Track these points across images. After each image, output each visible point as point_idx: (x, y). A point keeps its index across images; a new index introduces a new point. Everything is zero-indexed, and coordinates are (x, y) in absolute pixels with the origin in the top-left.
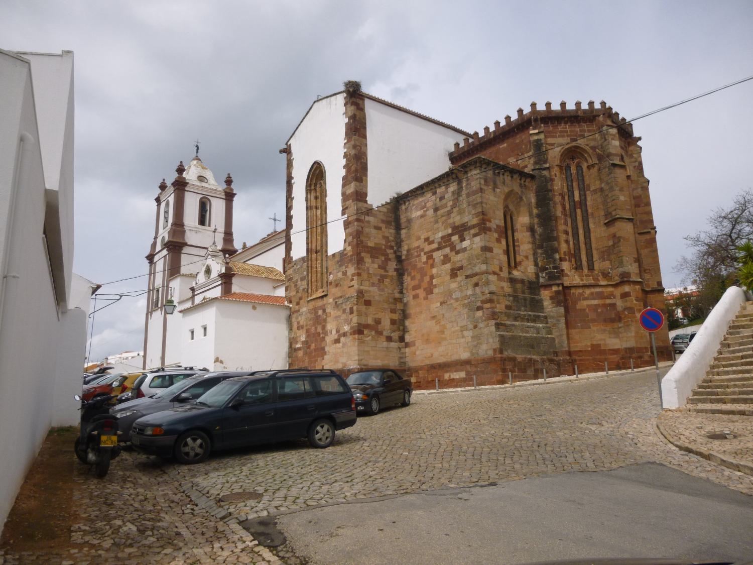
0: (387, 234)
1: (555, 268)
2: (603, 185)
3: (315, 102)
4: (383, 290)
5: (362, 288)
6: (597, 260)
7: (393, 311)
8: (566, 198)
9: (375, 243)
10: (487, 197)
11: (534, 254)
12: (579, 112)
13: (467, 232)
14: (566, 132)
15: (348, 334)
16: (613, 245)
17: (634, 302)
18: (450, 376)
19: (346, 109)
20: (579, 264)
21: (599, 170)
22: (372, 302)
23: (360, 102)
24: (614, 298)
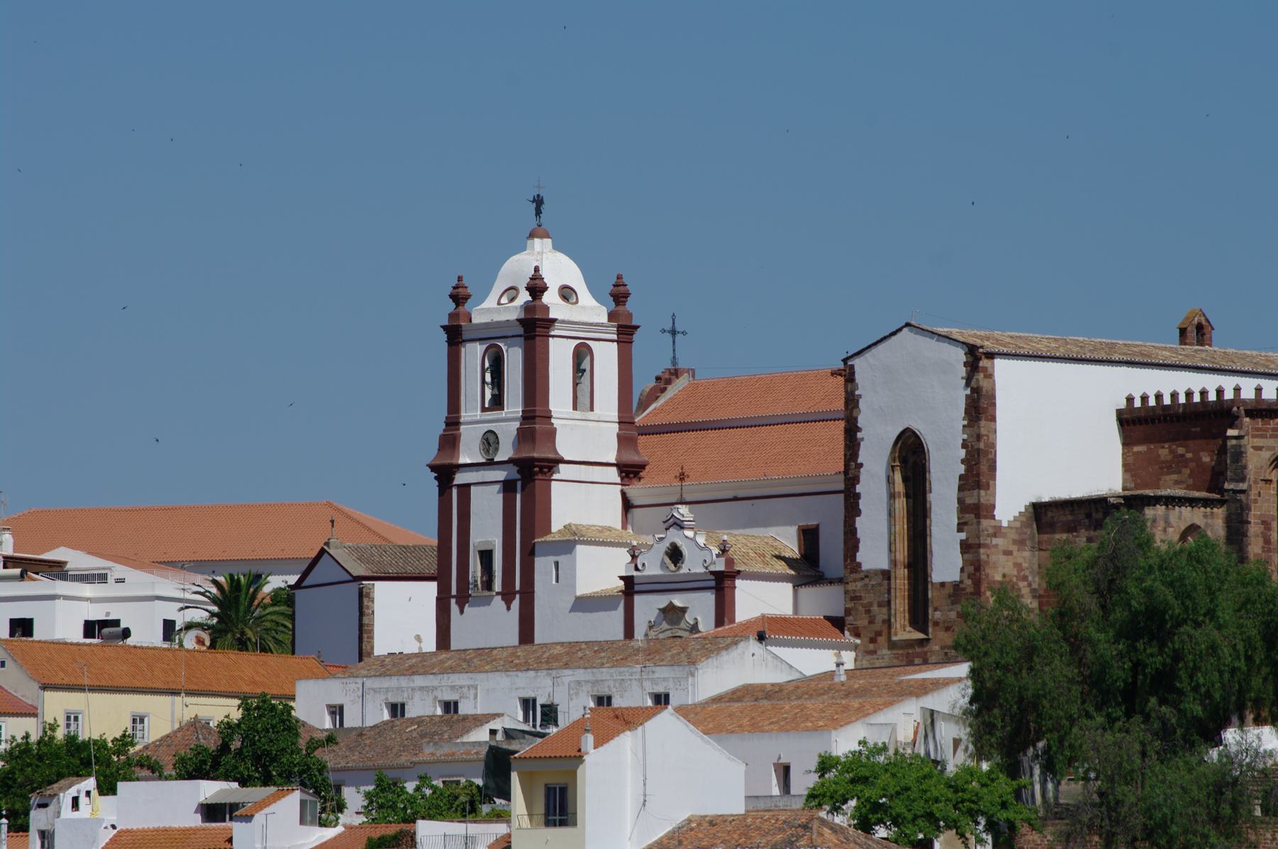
0: (1020, 560)
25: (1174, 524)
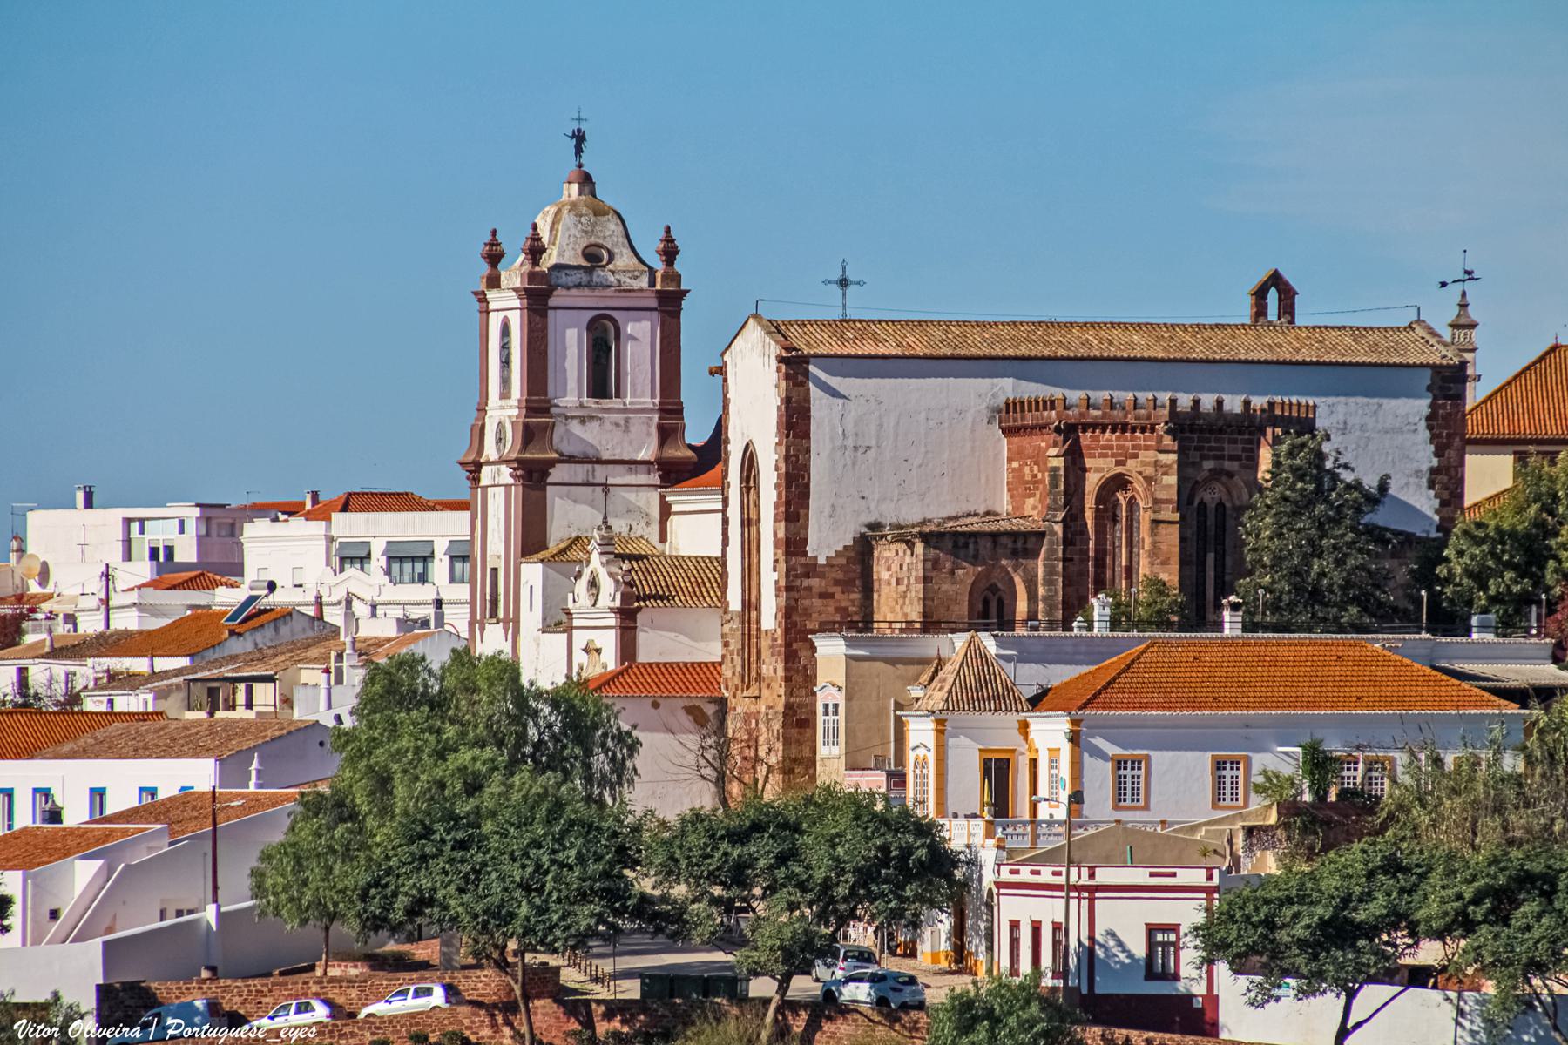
0: (844, 604)
5: (792, 700)
10: (936, 587)
14: (1111, 448)
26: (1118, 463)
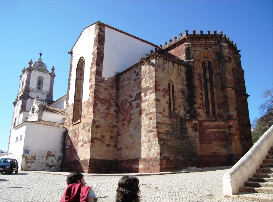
0: (111, 93)
1: (194, 112)
2: (220, 71)
3: (85, 29)
4: (107, 121)
5: (95, 119)
6: (217, 109)
7: (111, 132)
8: (202, 77)
9: (104, 97)
10: (159, 73)
11: (184, 104)
12: (209, 36)
13: (148, 92)
14: (203, 45)
15: (87, 142)
16: (225, 101)
17: (234, 130)
18: (136, 166)
19: (96, 32)
20: (208, 110)
21: (219, 64)
22: (100, 126)
23: (103, 28)
24: (225, 128)
25: (167, 69)
26: (205, 49)
